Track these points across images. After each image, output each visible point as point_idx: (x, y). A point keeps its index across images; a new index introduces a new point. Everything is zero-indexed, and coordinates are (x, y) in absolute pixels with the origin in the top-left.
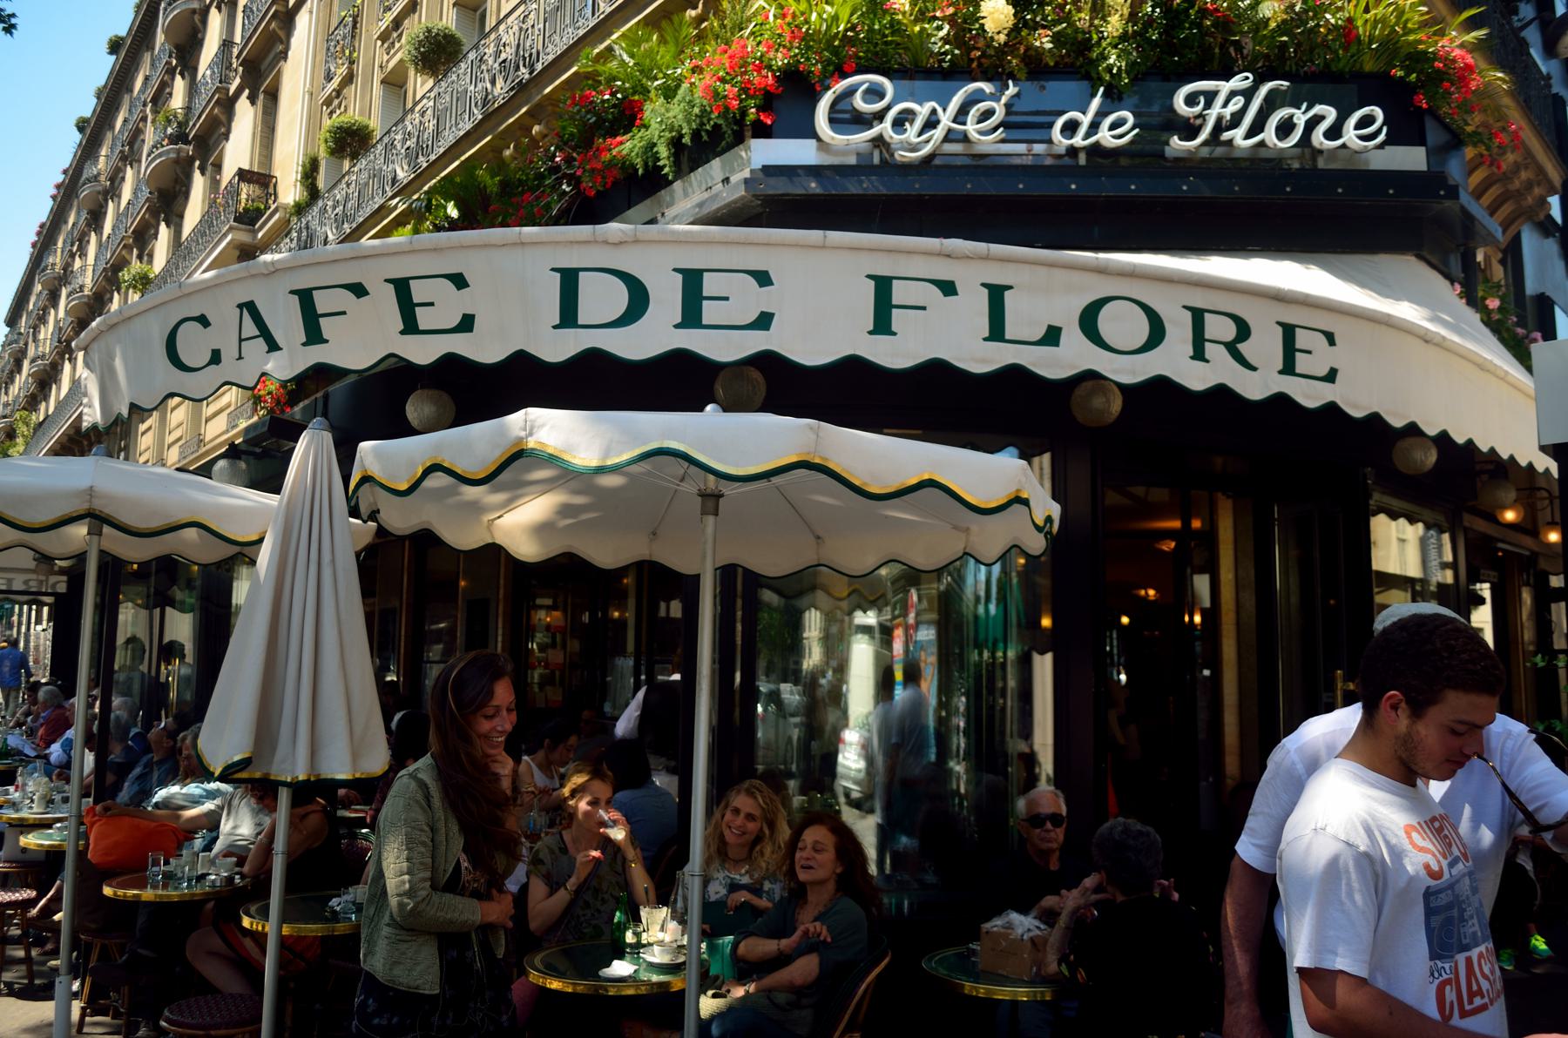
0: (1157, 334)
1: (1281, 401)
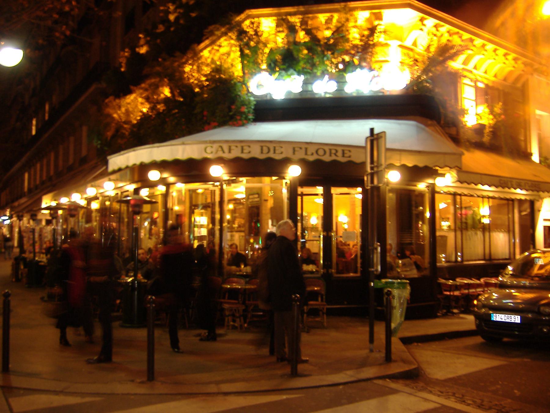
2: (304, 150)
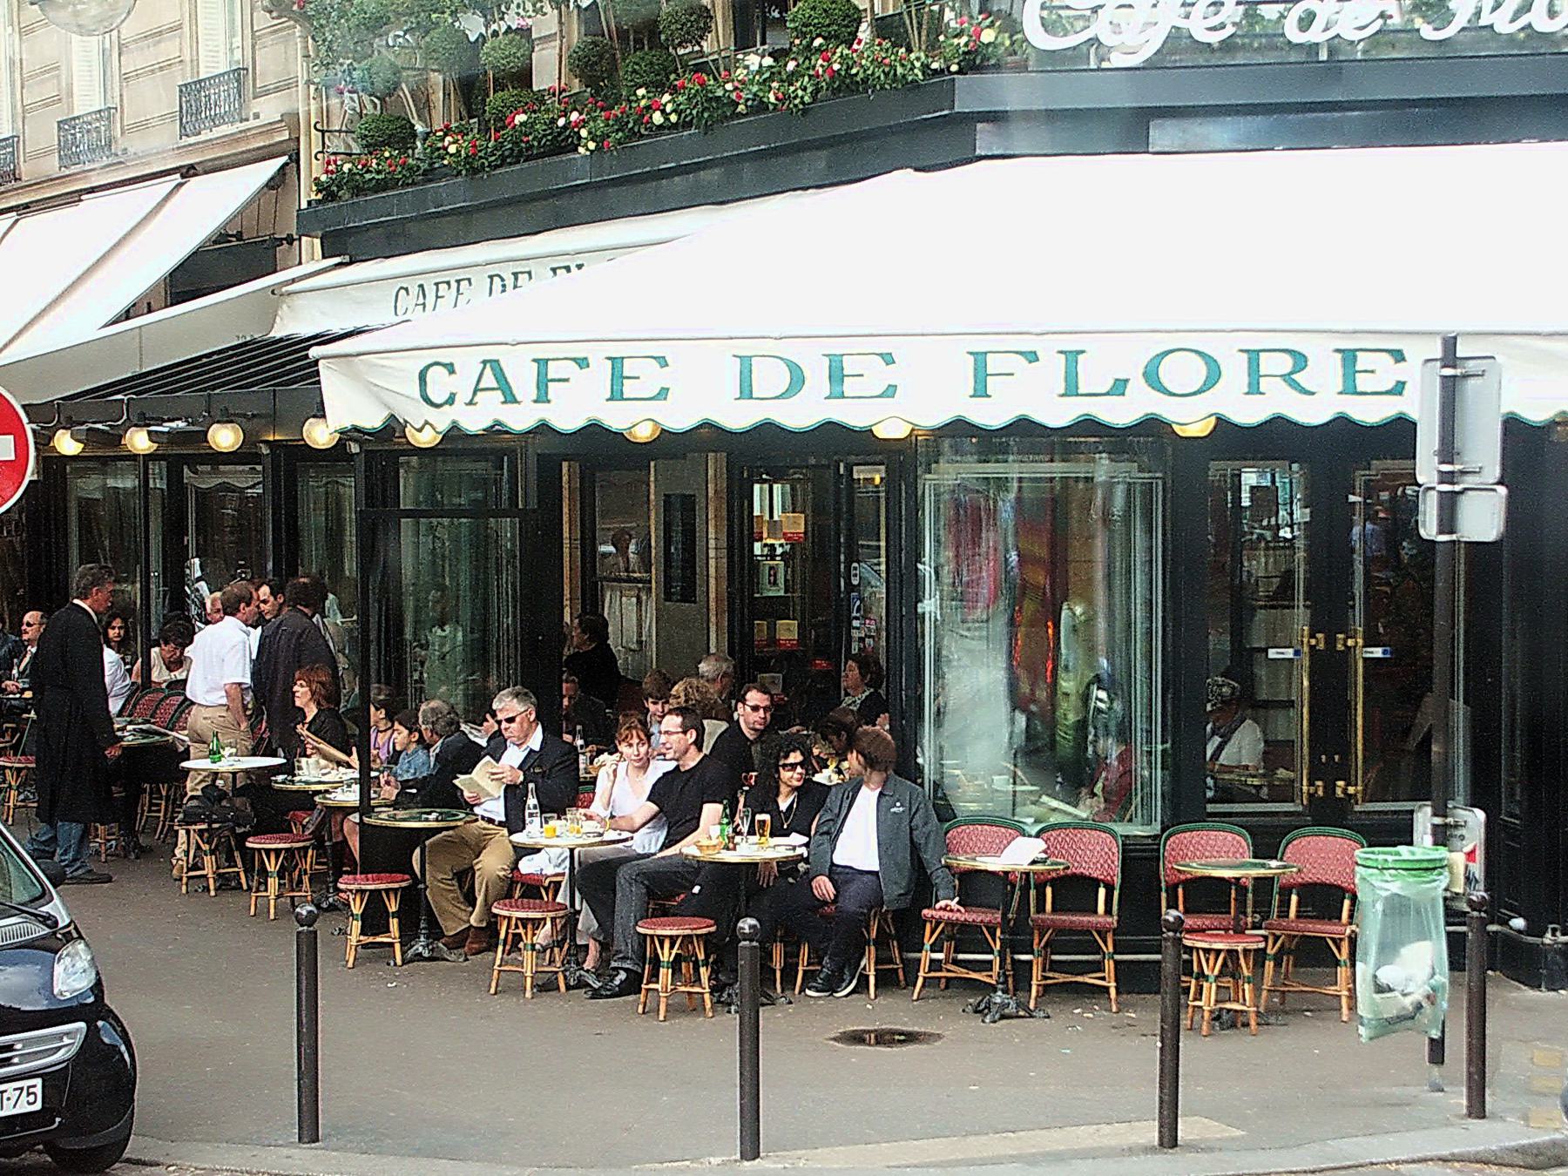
0: (1214, 375)
1: (1342, 423)
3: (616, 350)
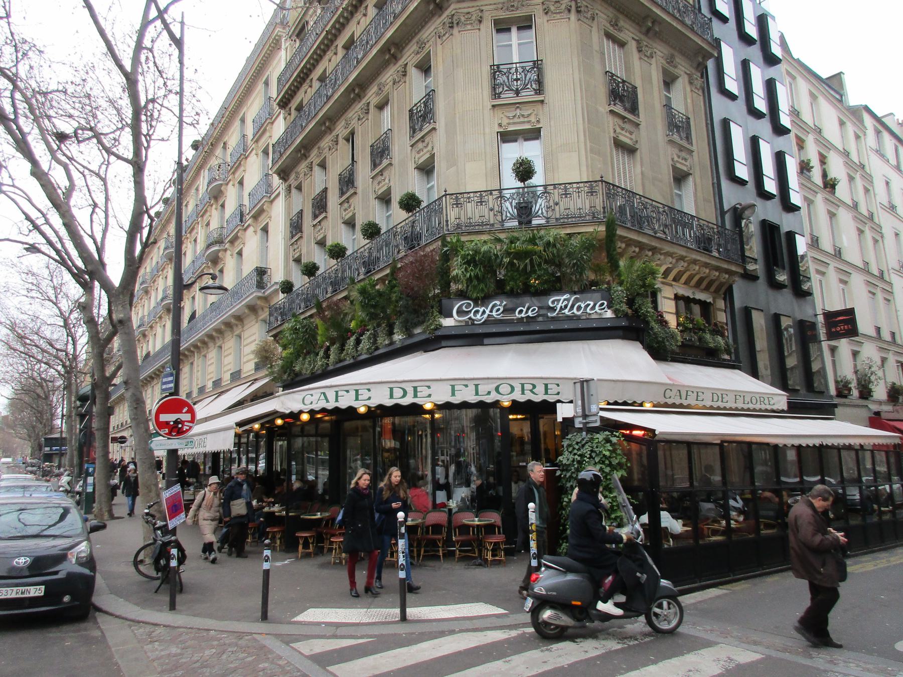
2: (472, 388)
3: (357, 387)
